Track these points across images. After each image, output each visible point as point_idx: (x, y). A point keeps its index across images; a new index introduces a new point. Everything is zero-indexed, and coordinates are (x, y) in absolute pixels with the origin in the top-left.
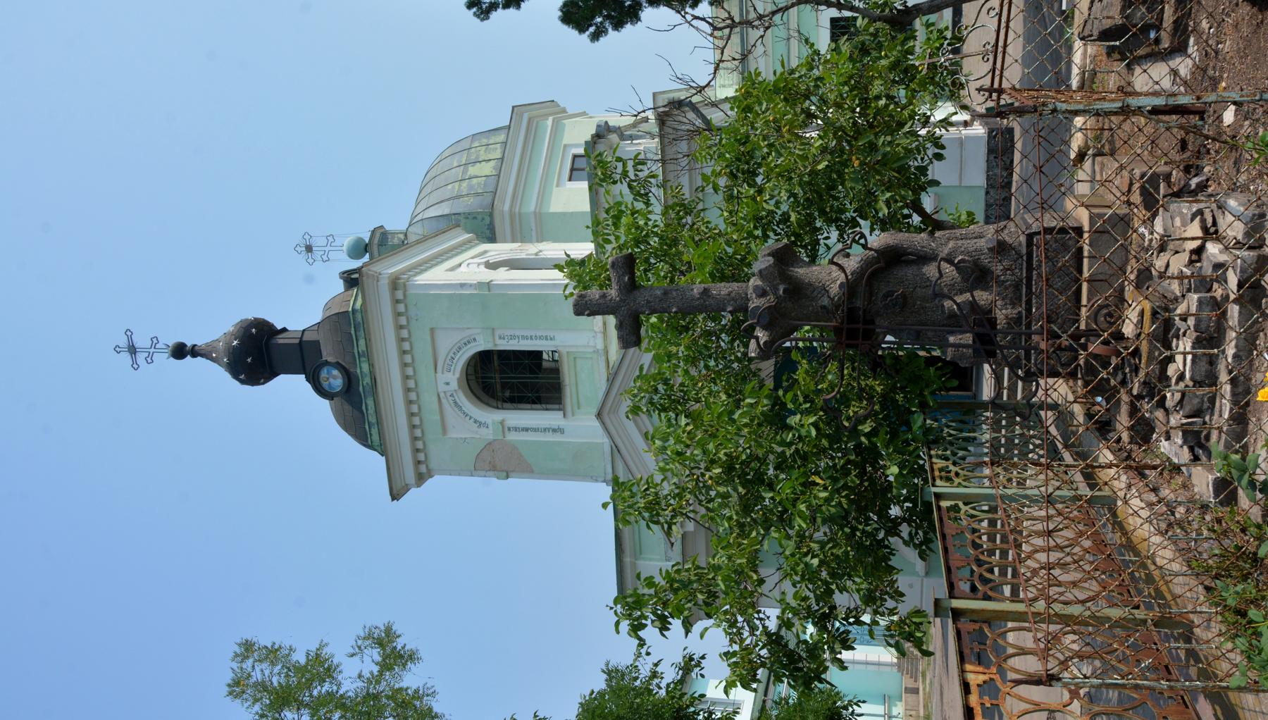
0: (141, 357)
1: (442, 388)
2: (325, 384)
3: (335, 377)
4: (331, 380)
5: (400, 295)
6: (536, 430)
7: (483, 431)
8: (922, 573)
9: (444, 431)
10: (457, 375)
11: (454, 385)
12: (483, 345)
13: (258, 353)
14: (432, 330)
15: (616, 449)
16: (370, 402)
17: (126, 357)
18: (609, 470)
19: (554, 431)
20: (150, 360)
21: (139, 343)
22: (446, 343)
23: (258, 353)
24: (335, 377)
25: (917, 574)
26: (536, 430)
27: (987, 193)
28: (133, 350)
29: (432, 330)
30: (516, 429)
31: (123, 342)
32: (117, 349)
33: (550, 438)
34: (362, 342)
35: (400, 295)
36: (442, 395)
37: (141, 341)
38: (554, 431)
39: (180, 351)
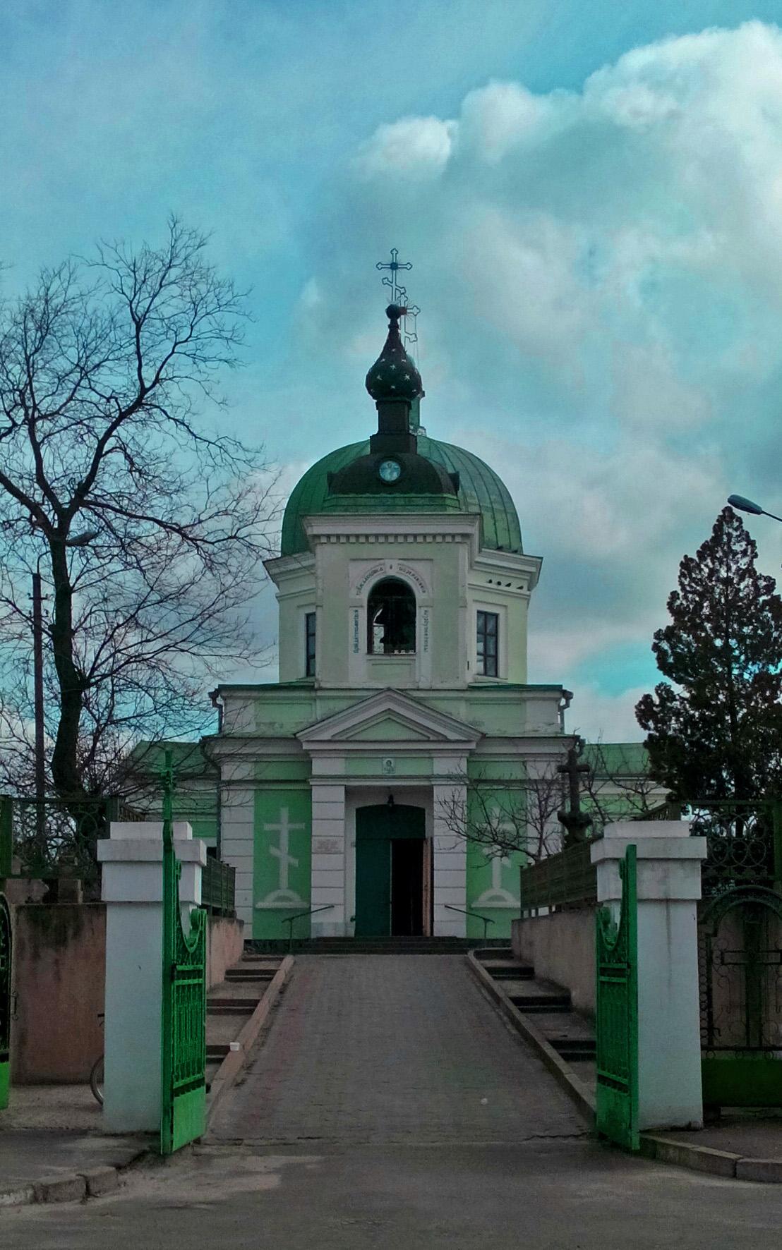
0: (387, 273)
1: (388, 562)
2: (385, 465)
3: (391, 473)
5: (458, 539)
6: (356, 630)
7: (354, 591)
8: (260, 905)
12: (420, 596)
13: (394, 386)
16: (373, 502)
17: (388, 259)
18: (328, 686)
19: (356, 646)
20: (385, 282)
21: (401, 273)
22: (420, 568)
23: (394, 386)
24: (391, 473)
25: (255, 901)
26: (356, 630)
28: (394, 266)
30: (357, 616)
31: (402, 259)
32: (394, 251)
33: (352, 641)
34: (421, 502)
35: (458, 539)
37: (402, 277)
39: (394, 313)
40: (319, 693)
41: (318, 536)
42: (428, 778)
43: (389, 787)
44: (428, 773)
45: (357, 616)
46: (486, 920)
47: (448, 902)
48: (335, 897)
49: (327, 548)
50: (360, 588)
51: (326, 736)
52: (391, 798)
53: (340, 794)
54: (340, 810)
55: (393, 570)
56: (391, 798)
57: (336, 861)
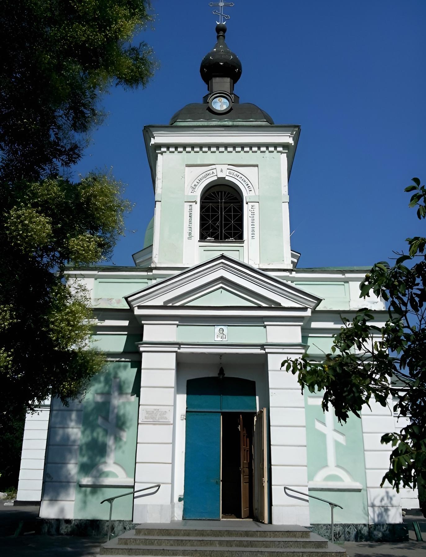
1: (219, 167)
3: (221, 106)
4: (220, 104)
6: (190, 222)
9: (188, 166)
10: (227, 178)
11: (221, 175)
12: (246, 195)
14: (257, 166)
15: (185, 271)
19: (190, 234)
24: (221, 106)
26: (190, 222)
27: (365, 525)
29: (257, 166)
30: (191, 210)
36: (213, 167)
38: (190, 234)
40: (155, 272)
41: (158, 146)
42: (262, 346)
43: (221, 355)
44: (263, 342)
45: (191, 210)
46: (333, 505)
47: (287, 482)
48: (160, 474)
49: (167, 155)
50: (194, 188)
51: (159, 302)
52: (221, 371)
53: (170, 361)
54: (170, 378)
55: (223, 172)
56: (221, 371)
57: (164, 432)
